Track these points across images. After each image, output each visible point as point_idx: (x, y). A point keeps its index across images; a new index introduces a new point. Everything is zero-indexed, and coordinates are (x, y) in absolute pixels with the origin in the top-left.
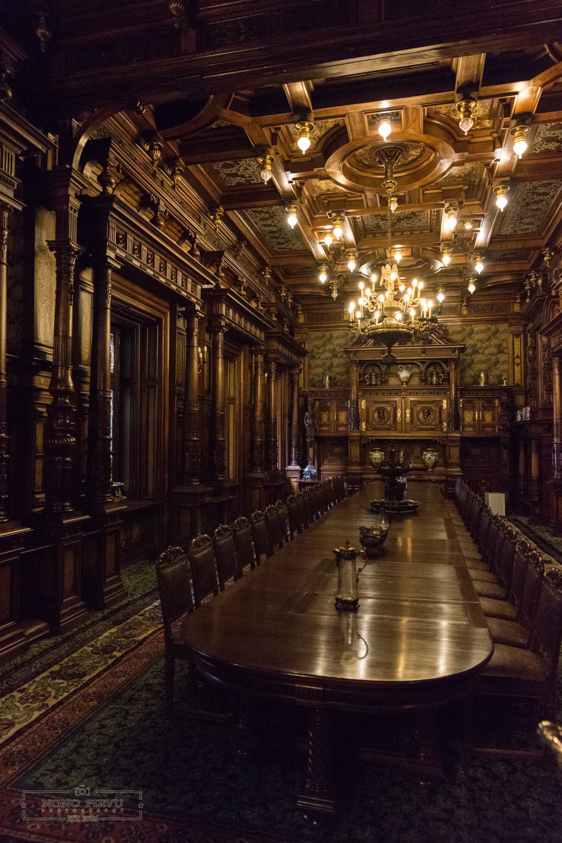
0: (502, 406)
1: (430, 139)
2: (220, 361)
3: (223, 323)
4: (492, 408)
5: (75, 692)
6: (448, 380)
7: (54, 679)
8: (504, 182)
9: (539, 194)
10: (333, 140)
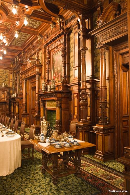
0: (7, 93)
4: (5, 94)
8: (18, 31)
9: (24, 36)
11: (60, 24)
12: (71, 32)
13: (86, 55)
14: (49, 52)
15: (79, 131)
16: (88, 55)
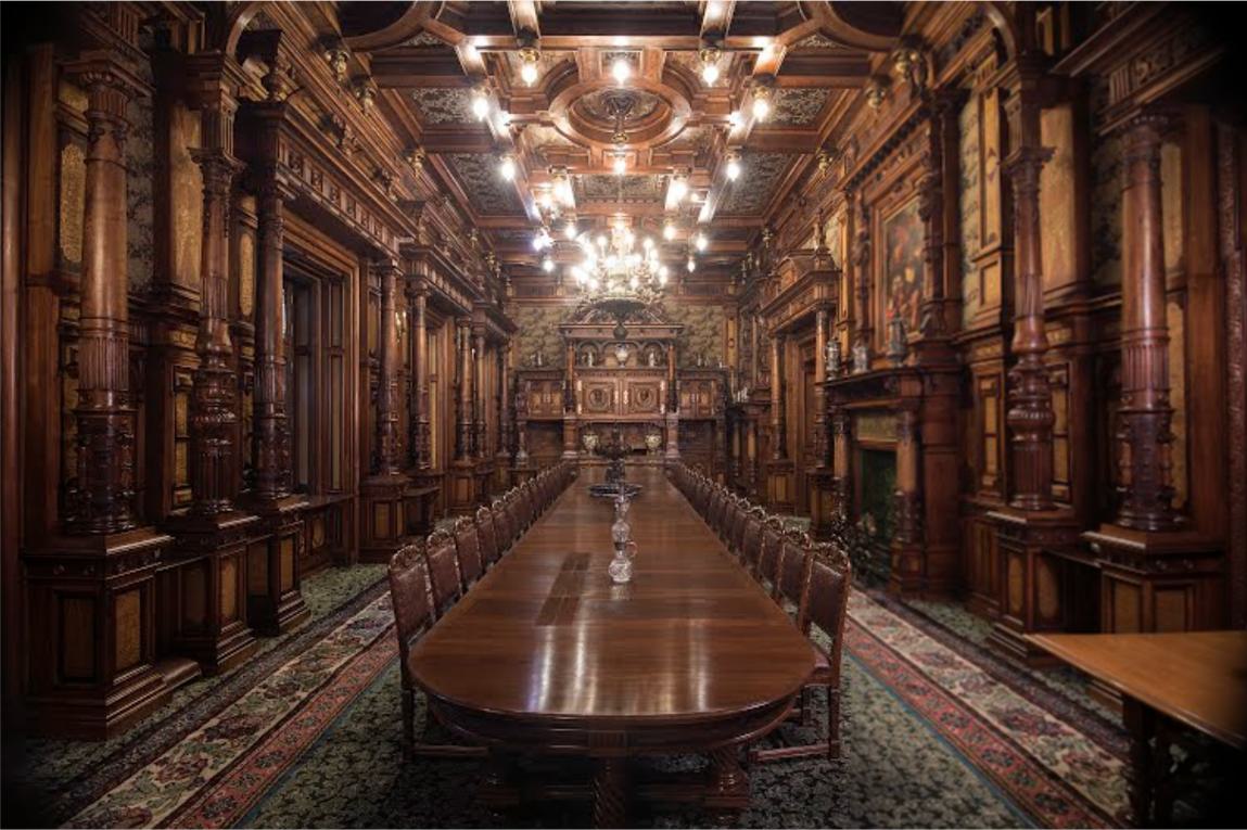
1: (667, 91)
2: (422, 331)
3: (425, 286)
5: (243, 756)
6: (667, 363)
7: (210, 739)
9: (764, 169)
10: (562, 79)
11: (911, 74)
12: (964, 97)
13: (1041, 186)
14: (865, 210)
15: (1008, 551)
16: (1055, 187)
